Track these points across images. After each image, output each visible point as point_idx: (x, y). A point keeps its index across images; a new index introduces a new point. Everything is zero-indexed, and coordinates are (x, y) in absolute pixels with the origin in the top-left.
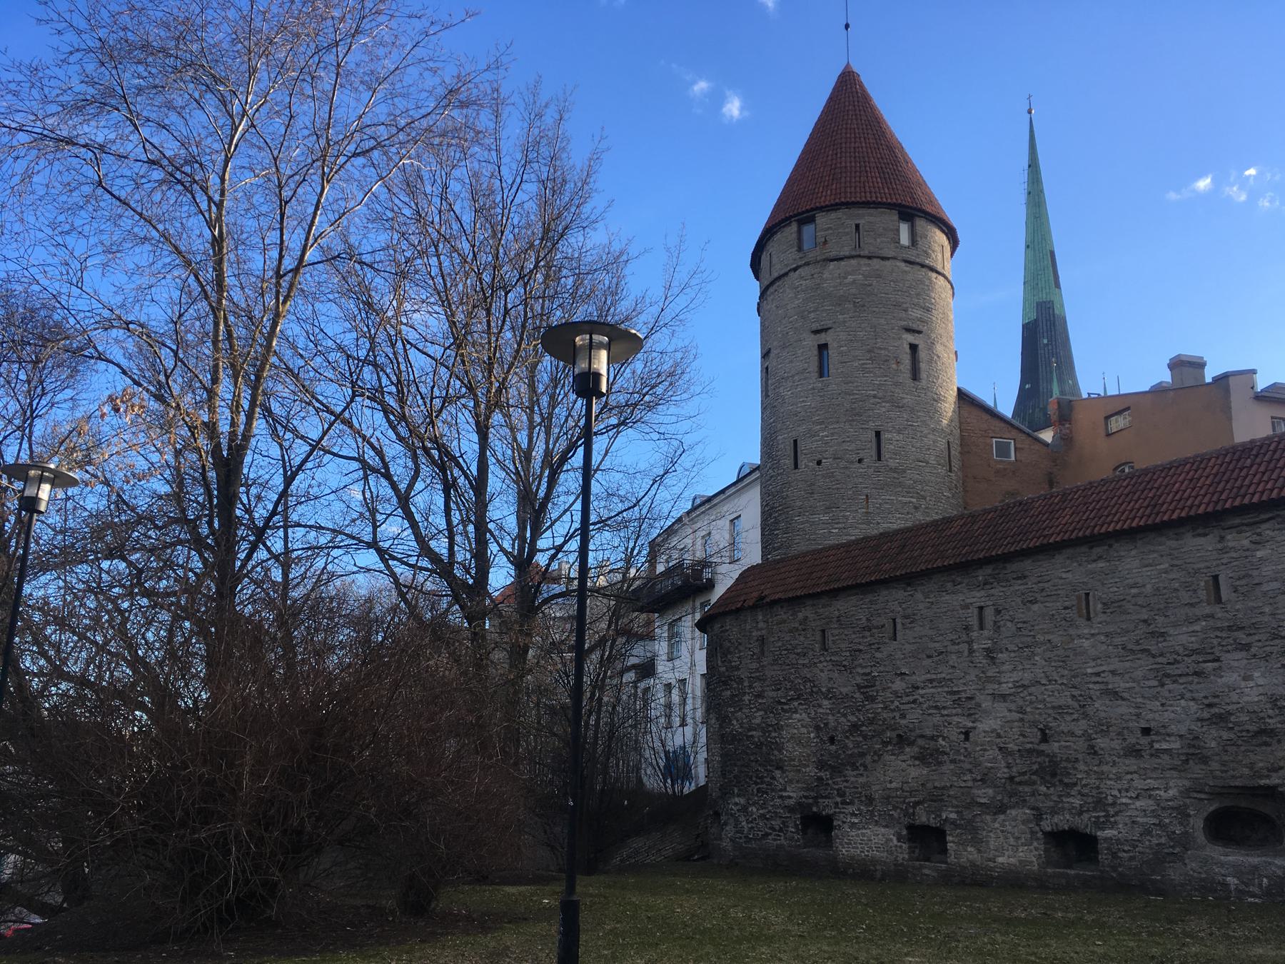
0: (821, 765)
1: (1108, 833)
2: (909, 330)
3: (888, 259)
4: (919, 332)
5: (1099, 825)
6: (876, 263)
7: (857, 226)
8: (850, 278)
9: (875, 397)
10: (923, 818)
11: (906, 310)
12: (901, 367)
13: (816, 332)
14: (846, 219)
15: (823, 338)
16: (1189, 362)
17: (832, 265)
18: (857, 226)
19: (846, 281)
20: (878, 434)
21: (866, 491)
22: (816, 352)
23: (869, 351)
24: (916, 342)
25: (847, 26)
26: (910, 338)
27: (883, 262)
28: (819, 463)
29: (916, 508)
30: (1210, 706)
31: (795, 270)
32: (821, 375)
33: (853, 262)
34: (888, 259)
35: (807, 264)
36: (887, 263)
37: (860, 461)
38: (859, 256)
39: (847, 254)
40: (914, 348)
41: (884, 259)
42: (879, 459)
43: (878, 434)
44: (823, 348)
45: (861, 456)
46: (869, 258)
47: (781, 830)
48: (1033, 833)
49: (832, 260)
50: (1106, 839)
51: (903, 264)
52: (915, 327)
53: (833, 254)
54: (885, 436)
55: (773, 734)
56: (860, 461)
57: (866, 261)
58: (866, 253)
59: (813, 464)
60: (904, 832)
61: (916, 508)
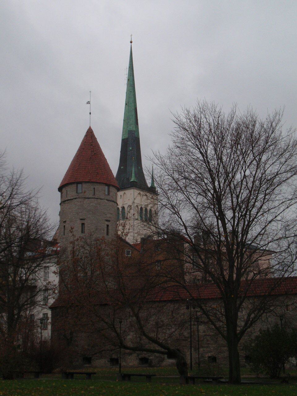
1: (151, 358)
3: (102, 199)
5: (149, 356)
6: (99, 200)
7: (94, 188)
10: (114, 356)
11: (106, 215)
12: (104, 232)
13: (81, 219)
14: (92, 187)
15: (83, 222)
17: (87, 200)
18: (94, 188)
22: (81, 225)
24: (108, 224)
25: (90, 113)
26: (107, 223)
27: (101, 200)
31: (75, 199)
32: (82, 233)
33: (93, 199)
34: (102, 199)
35: (79, 198)
38: (94, 198)
40: (108, 226)
41: (101, 199)
44: (83, 224)
46: (97, 199)
47: (77, 361)
48: (137, 359)
50: (150, 359)
51: (106, 201)
53: (87, 196)
55: (76, 338)
58: (96, 197)
60: (109, 360)
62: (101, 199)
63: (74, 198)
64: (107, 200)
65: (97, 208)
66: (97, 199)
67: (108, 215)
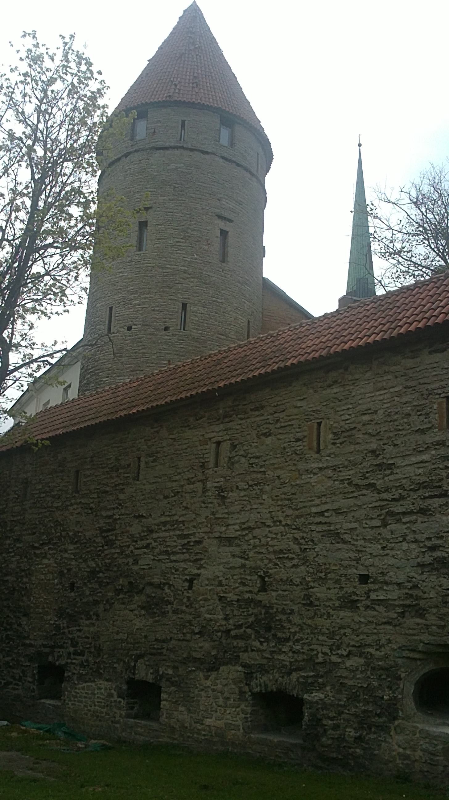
0: (61, 614)
1: (317, 696)
2: (220, 217)
3: (208, 153)
4: (231, 221)
5: (307, 686)
6: (196, 155)
7: (183, 122)
10: (144, 673)
17: (158, 153)
18: (183, 122)
19: (168, 168)
20: (184, 306)
21: (169, 357)
22: (137, 229)
26: (222, 224)
28: (129, 329)
30: (433, 548)
31: (126, 155)
32: (140, 249)
33: (177, 152)
34: (208, 153)
36: (207, 157)
37: (166, 329)
39: (172, 144)
40: (224, 234)
41: (204, 152)
43: (184, 306)
44: (143, 225)
45: (167, 325)
46: (191, 150)
47: (20, 679)
48: (242, 693)
49: (157, 149)
50: (311, 702)
51: (221, 160)
52: (226, 214)
53: (160, 144)
55: (25, 580)
57: (189, 153)
59: (124, 330)
60: (125, 687)
62: (204, 152)
63: (122, 156)
64: (223, 158)
65: (188, 176)
66: (191, 150)
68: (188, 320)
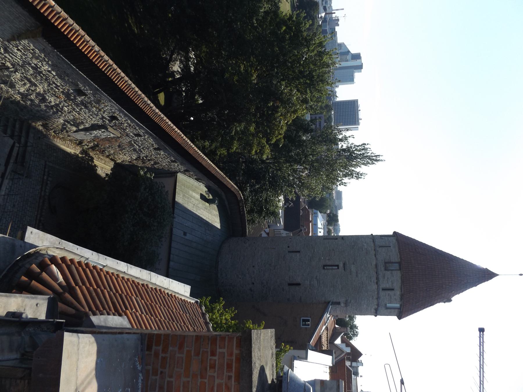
2: (344, 264)
8: (365, 245)
9: (314, 251)
11: (353, 264)
16: (339, 385)
20: (299, 252)
23: (333, 250)
24: (340, 268)
26: (341, 265)
29: (270, 265)
33: (373, 245)
36: (374, 257)
42: (289, 252)
43: (299, 252)
46: (375, 250)
54: (298, 254)
56: (288, 247)
57: (373, 248)
61: (270, 265)
67: (353, 268)
68: (292, 253)
